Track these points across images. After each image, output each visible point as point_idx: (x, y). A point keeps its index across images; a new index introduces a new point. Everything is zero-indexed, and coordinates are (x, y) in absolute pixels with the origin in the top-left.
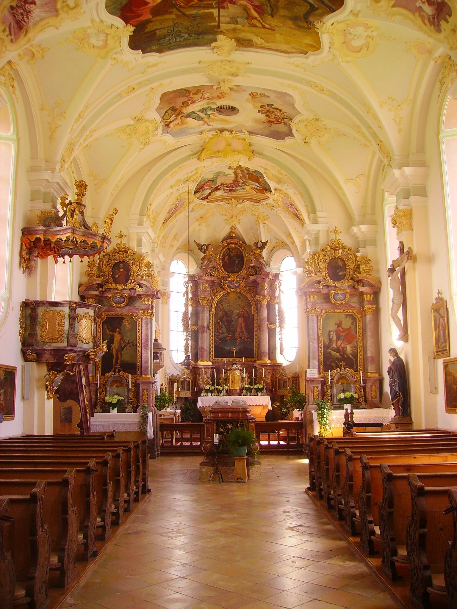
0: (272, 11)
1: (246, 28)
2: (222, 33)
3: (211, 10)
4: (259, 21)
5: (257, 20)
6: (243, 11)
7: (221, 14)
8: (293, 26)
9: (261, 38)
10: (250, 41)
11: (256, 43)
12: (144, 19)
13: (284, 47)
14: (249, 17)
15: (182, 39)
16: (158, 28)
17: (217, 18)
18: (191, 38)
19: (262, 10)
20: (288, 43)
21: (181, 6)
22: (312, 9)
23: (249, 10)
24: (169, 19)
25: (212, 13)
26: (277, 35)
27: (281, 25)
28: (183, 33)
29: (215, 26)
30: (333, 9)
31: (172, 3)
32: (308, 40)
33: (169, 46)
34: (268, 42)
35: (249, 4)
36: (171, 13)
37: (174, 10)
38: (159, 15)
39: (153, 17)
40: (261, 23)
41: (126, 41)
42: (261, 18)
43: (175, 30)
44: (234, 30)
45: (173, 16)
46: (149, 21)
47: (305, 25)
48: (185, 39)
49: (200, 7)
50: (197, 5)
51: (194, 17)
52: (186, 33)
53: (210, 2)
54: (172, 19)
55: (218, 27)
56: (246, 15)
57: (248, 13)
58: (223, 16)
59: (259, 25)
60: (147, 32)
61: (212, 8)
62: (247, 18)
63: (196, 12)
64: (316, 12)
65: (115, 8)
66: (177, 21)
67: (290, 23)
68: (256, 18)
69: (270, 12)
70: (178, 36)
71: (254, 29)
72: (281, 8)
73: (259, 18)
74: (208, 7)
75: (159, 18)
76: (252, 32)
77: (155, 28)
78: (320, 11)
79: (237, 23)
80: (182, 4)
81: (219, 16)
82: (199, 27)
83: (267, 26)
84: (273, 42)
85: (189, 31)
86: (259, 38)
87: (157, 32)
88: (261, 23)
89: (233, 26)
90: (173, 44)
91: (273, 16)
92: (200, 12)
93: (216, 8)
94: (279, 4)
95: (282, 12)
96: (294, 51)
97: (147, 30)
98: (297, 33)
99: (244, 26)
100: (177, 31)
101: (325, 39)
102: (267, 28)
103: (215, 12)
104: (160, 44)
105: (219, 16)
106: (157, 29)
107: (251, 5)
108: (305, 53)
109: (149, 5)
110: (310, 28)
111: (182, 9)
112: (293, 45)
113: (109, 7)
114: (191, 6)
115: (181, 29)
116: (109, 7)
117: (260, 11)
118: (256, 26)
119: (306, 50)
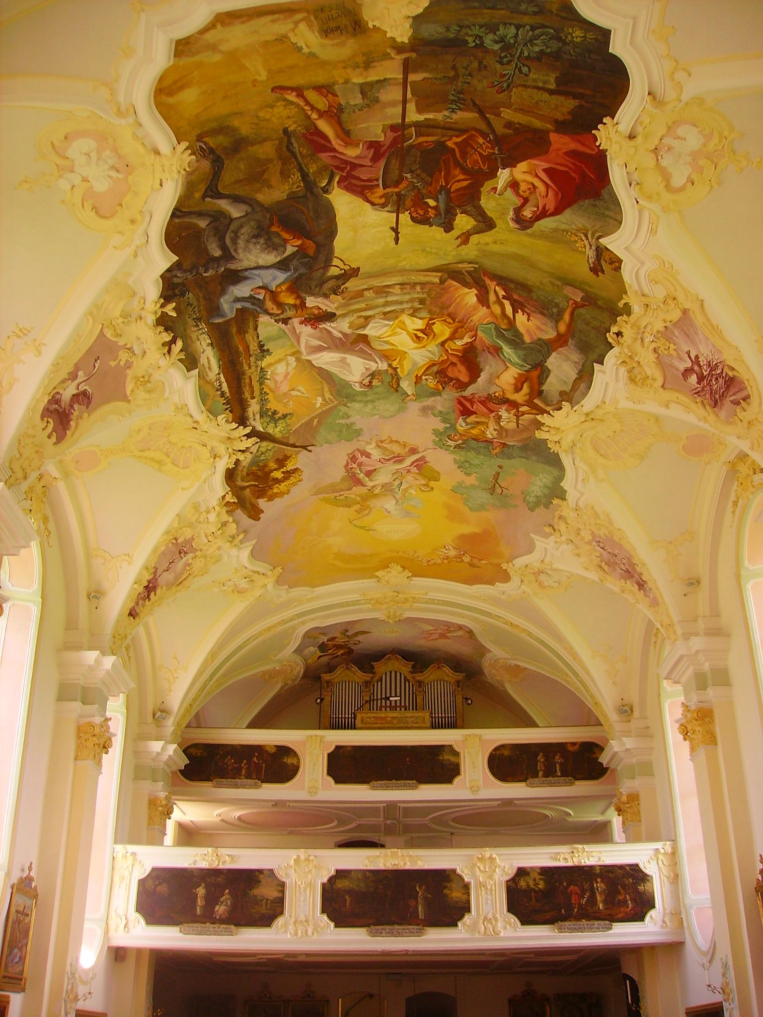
0: (290, 143)
1: (338, 75)
2: (400, 48)
3: (421, 118)
4: (313, 108)
5: (318, 111)
6: (351, 128)
7: (399, 109)
8: (236, 123)
9: (300, 49)
10: (326, 32)
11: (310, 27)
12: (566, 139)
13: (237, 37)
14: (335, 114)
15: (501, 31)
16: (546, 96)
17: (409, 95)
18: (476, 31)
19: (311, 142)
20: (233, 58)
21: (484, 135)
22: (213, 191)
23: (338, 137)
24: (516, 110)
25: (420, 111)
26: (263, 76)
27: (261, 114)
28: (494, 53)
29: (415, 71)
30: (178, 217)
31: (499, 150)
32: (189, 98)
33: (538, 20)
34: (282, 39)
35: (341, 149)
36: (509, 125)
37: (500, 129)
38: (535, 131)
39: (547, 132)
40: (307, 103)
41: (629, 111)
42: (309, 117)
43: (509, 70)
44: (367, 65)
45: (508, 114)
46: (561, 127)
47: (211, 142)
48: (492, 28)
49: (443, 128)
50: (450, 133)
51: (461, 101)
52: (486, 51)
53: (421, 139)
54: (509, 106)
55: (407, 67)
56: (344, 117)
57: (340, 123)
58: (393, 104)
59: (312, 96)
60: (575, 96)
61: (417, 125)
62: (341, 109)
63: (454, 116)
64: (203, 187)
65: (608, 209)
66: (502, 97)
67: (245, 128)
68: (321, 114)
69: (293, 140)
70: (507, 47)
71: (321, 78)
72: (272, 161)
73: (314, 116)
74: (428, 126)
75: (537, 124)
76: (324, 64)
77: (555, 100)
78: (197, 195)
79: (365, 90)
80: (481, 141)
81: (405, 102)
82: (454, 68)
83: (292, 97)
84: (266, 44)
85: (480, 54)
86: (306, 50)
87: (552, 86)
88: (307, 103)
89: (373, 76)
90: (526, 20)
91: (285, 131)
92: (446, 113)
93: (410, 126)
94: (279, 166)
95: (266, 150)
96: (210, 37)
97: (570, 104)
98: (222, 109)
99: (347, 82)
100: (510, 61)
101: (160, 135)
102: (292, 89)
103: (413, 116)
104: (559, 39)
105: (405, 102)
106: (551, 92)
107: (335, 150)
108: (182, 47)
109: (546, 165)
110: (199, 138)
111: (483, 126)
112: (217, 58)
113: (616, 220)
114: (464, 131)
115: (498, 66)
116: (616, 220)
117: (315, 138)
118: (318, 89)
119: (183, 61)
